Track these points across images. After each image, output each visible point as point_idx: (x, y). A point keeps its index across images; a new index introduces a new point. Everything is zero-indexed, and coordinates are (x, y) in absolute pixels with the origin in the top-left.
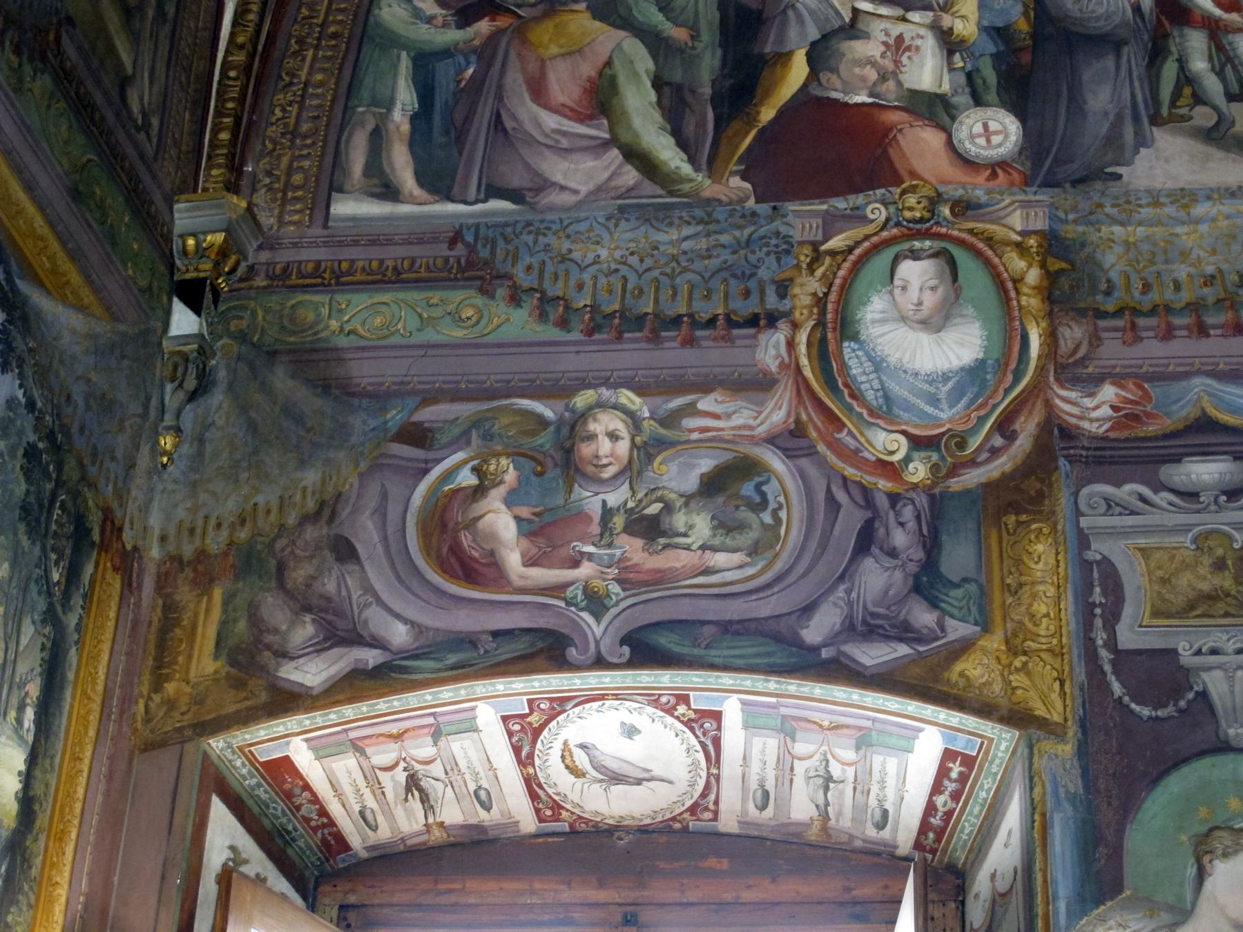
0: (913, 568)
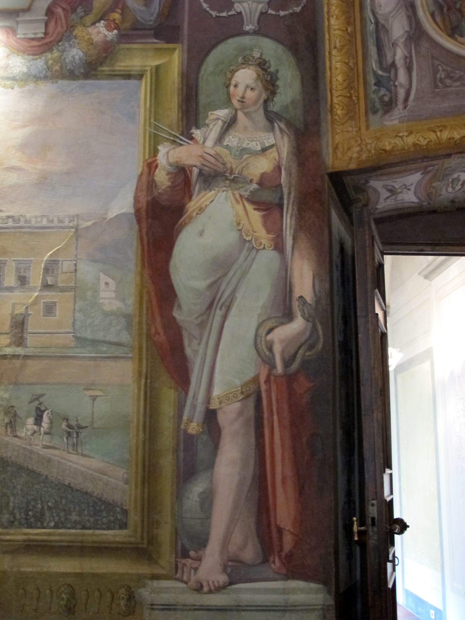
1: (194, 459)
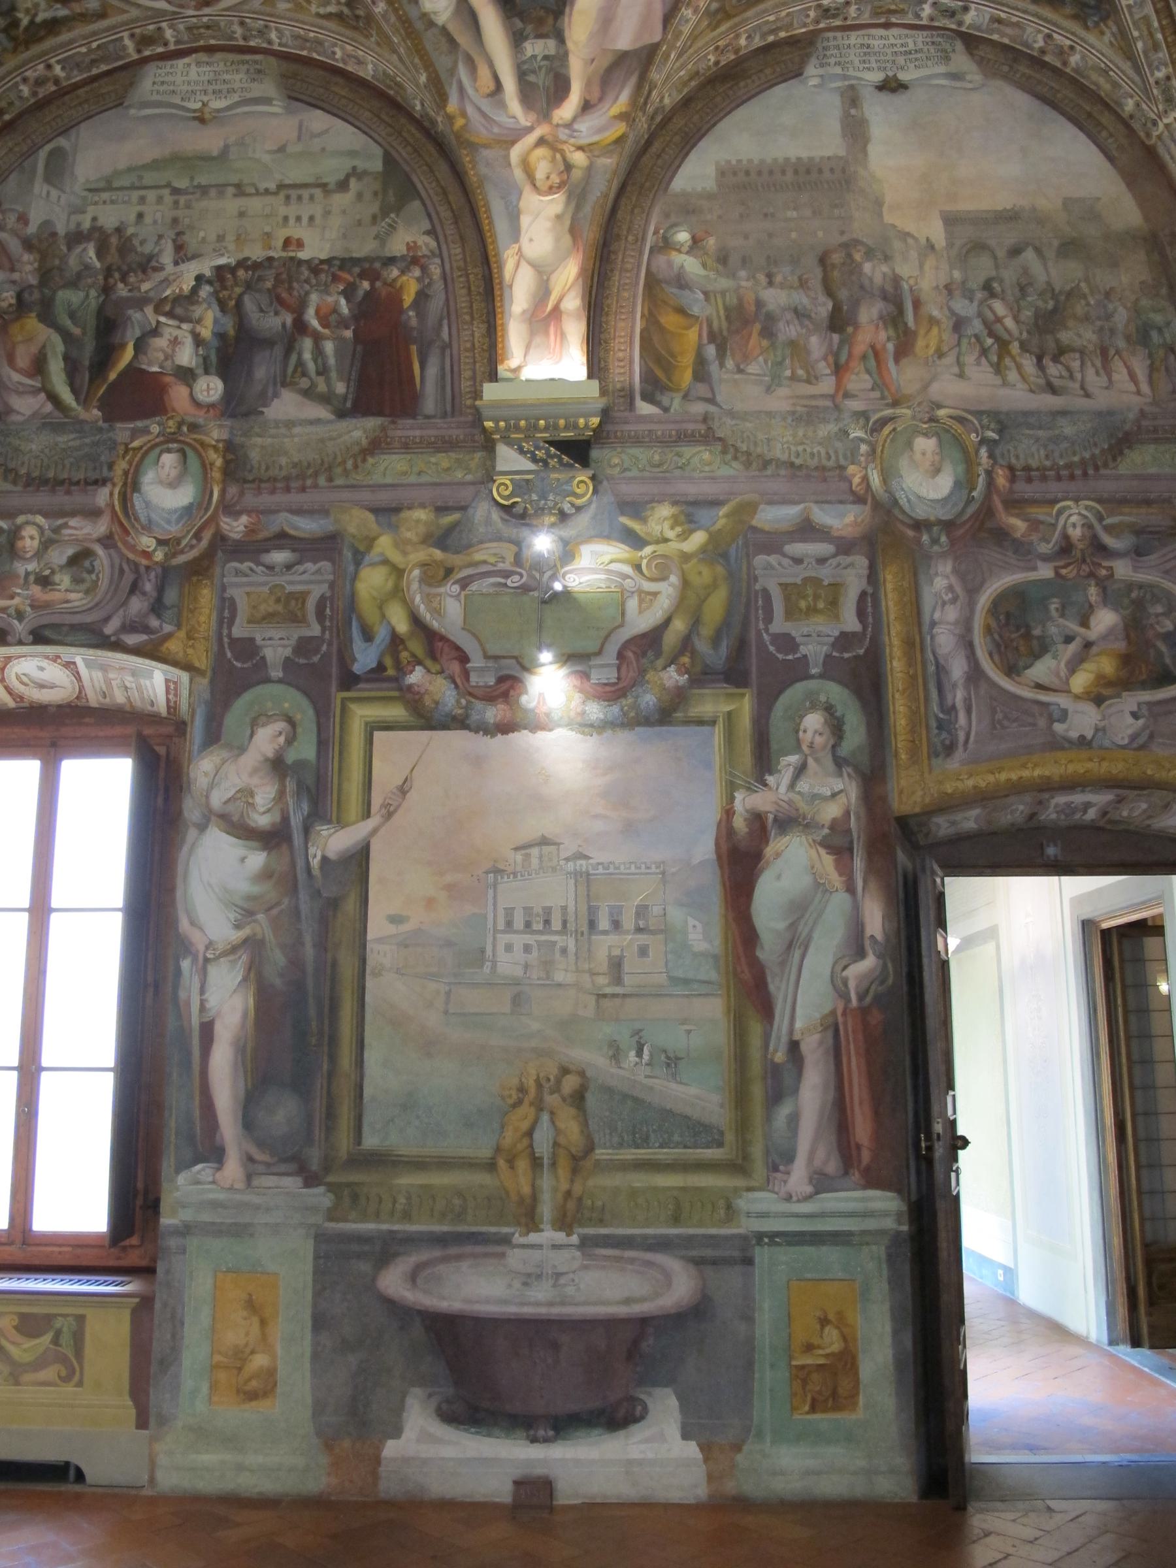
0: (152, 600)
1: (781, 1083)
